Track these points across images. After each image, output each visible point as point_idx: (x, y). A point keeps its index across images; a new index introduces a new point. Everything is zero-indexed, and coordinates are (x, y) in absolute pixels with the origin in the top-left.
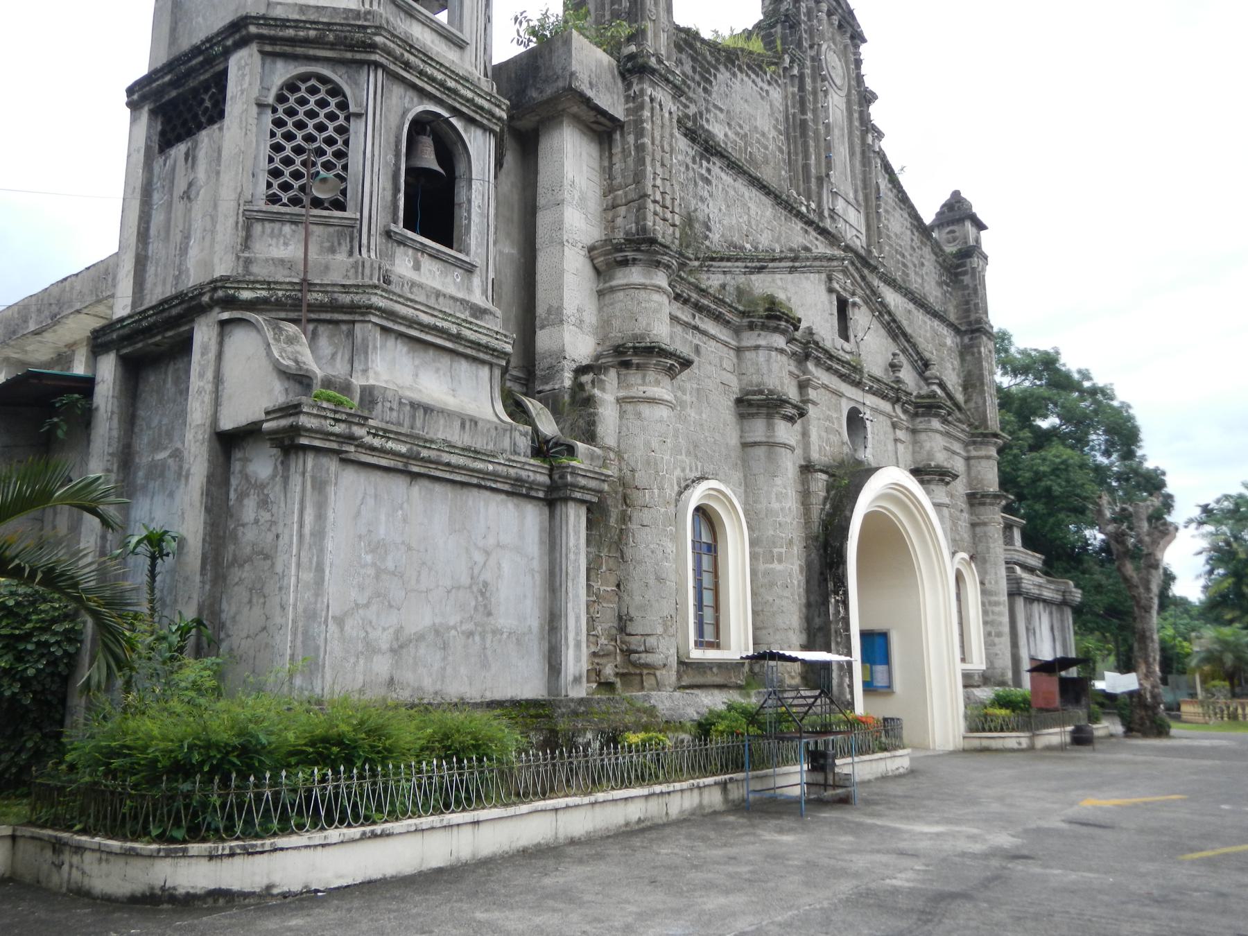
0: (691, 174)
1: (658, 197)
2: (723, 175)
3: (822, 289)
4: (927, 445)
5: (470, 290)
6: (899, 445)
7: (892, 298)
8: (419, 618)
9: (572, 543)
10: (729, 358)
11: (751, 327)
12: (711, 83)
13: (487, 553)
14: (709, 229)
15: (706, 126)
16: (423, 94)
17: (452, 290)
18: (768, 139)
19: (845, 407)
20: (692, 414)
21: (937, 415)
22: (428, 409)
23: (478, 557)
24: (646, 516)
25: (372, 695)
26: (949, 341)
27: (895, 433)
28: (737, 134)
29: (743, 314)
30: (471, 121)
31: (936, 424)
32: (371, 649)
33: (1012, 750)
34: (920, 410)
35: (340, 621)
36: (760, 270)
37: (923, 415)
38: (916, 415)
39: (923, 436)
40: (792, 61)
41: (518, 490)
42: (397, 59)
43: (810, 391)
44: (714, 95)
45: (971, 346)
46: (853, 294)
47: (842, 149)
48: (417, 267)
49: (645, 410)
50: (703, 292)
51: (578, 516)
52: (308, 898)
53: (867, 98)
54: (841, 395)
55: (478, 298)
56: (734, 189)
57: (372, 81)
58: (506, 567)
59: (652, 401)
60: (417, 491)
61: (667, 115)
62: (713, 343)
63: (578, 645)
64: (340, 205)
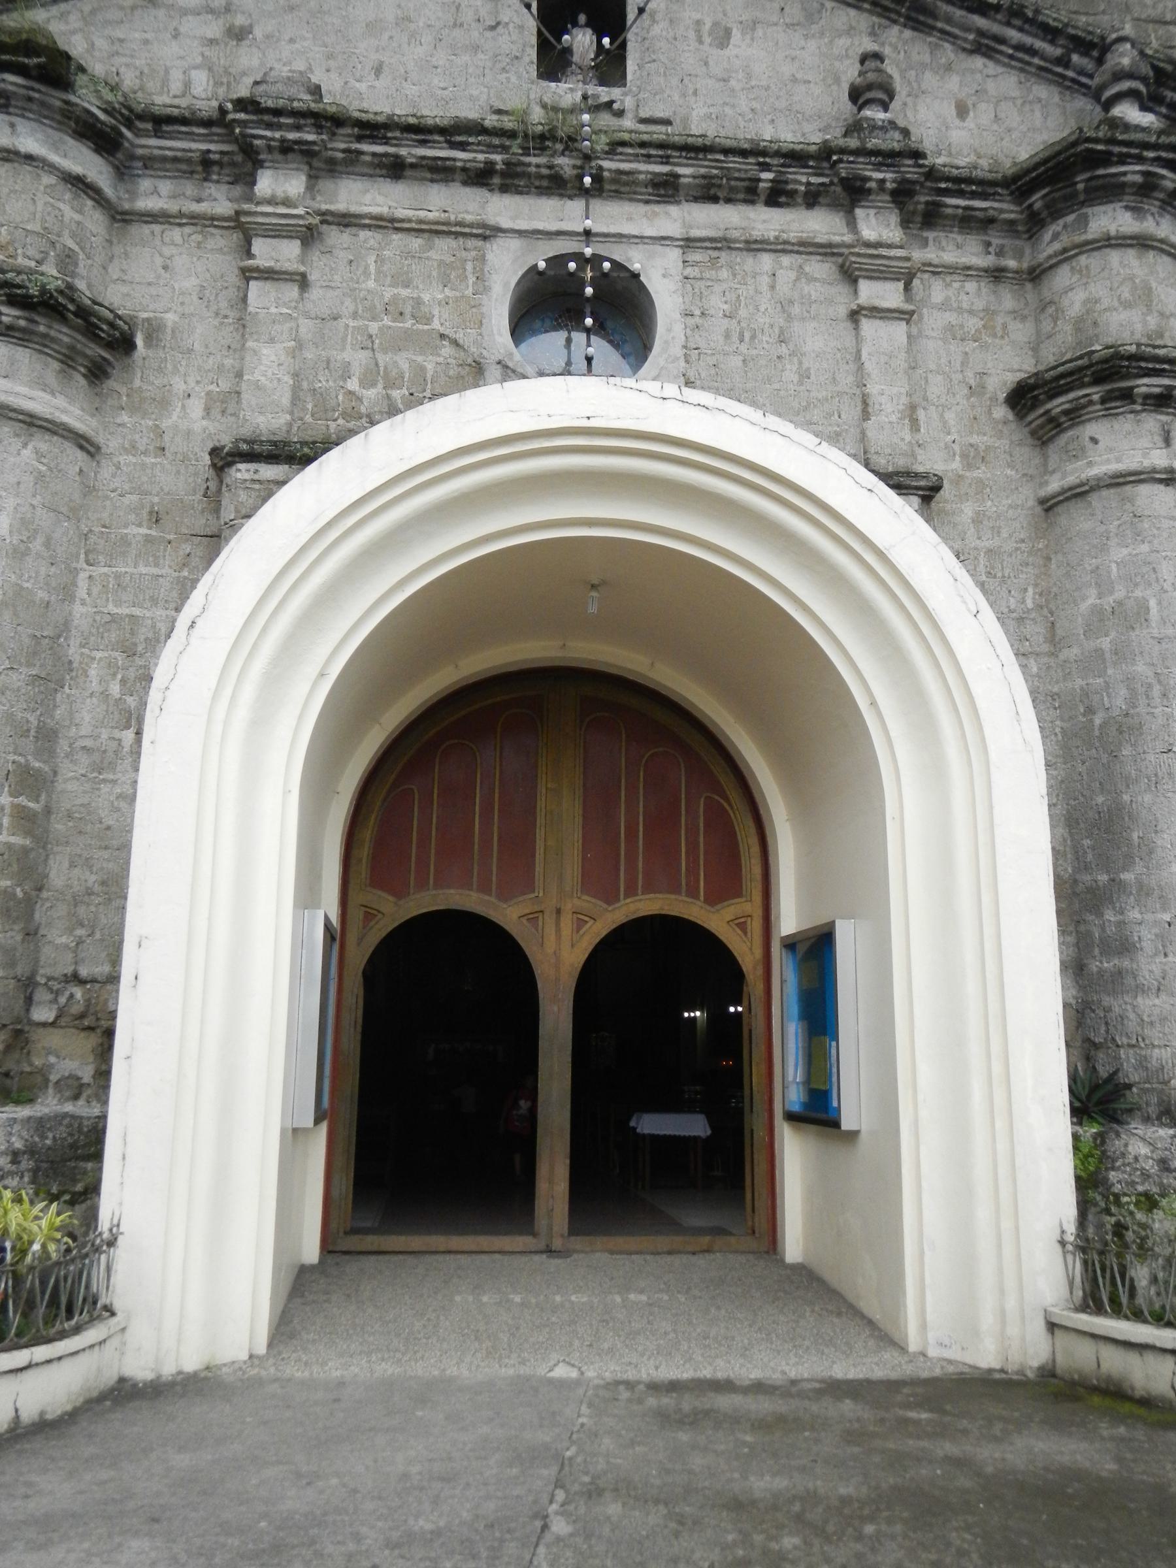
4: (1074, 303)
6: (868, 326)
21: (1110, 191)
27: (856, 292)
34: (1037, 200)
37: (1055, 211)
38: (1034, 224)
39: (1063, 277)
43: (259, 246)
54: (488, 233)
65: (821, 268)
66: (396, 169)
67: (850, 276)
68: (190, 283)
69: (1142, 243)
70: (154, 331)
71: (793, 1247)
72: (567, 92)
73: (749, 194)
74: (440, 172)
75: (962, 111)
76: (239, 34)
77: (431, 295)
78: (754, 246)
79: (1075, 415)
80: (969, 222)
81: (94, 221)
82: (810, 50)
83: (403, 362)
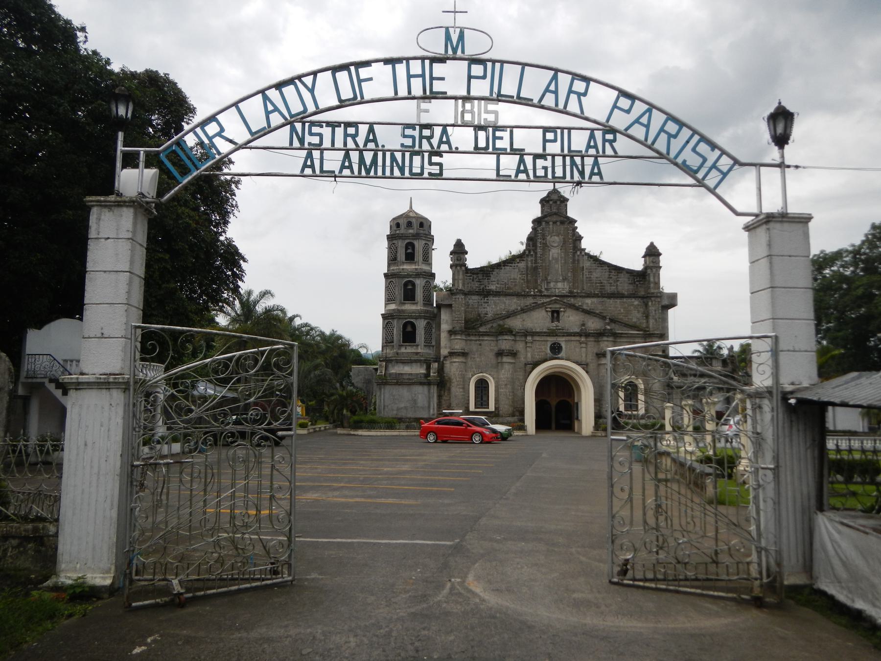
0: (480, 303)
1: (456, 319)
2: (494, 298)
3: (544, 311)
4: (602, 345)
5: (418, 349)
7: (589, 302)
8: (402, 405)
9: (432, 391)
10: (493, 344)
11: (499, 335)
12: (490, 276)
13: (415, 394)
14: (487, 314)
15: (487, 288)
16: (406, 318)
17: (414, 351)
18: (516, 279)
19: (549, 344)
20: (478, 359)
21: (605, 336)
22: (402, 374)
23: (414, 395)
24: (453, 385)
25: (394, 416)
26: (636, 303)
28: (502, 284)
29: (497, 332)
30: (416, 319)
31: (605, 338)
32: (393, 410)
33: (599, 436)
35: (387, 406)
36: (508, 318)
40: (530, 252)
41: (421, 384)
42: (399, 316)
44: (491, 278)
45: (648, 302)
46: (561, 308)
47: (557, 266)
48: (406, 348)
49: (454, 364)
50: (480, 332)
51: (434, 387)
52: (361, 436)
53: (580, 238)
54: (547, 341)
55: (419, 351)
56: (499, 300)
57: (395, 321)
58: (420, 396)
59: (455, 362)
60: (400, 387)
61: (460, 300)
62: (487, 342)
63: (434, 409)
64: (393, 342)
65: (578, 342)
66: (539, 335)
67: (581, 343)
68: (521, 346)
69: (608, 341)
70: (518, 351)
71: (576, 431)
72: (554, 324)
73: (571, 336)
74: (543, 335)
75: (593, 323)
76: (524, 320)
77: (543, 347)
78: (572, 341)
79: (600, 357)
80: (592, 336)
81: (513, 342)
82: (577, 318)
83: (541, 354)
